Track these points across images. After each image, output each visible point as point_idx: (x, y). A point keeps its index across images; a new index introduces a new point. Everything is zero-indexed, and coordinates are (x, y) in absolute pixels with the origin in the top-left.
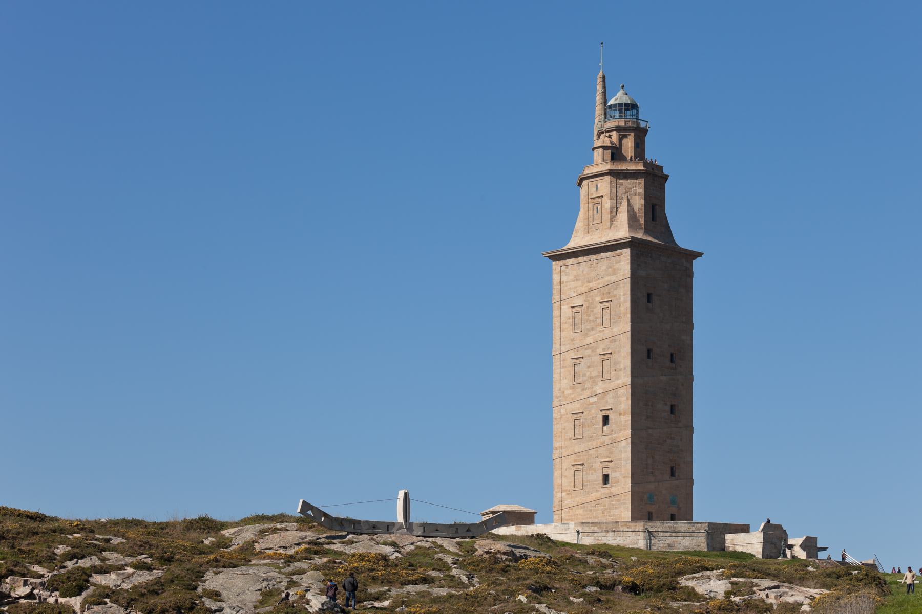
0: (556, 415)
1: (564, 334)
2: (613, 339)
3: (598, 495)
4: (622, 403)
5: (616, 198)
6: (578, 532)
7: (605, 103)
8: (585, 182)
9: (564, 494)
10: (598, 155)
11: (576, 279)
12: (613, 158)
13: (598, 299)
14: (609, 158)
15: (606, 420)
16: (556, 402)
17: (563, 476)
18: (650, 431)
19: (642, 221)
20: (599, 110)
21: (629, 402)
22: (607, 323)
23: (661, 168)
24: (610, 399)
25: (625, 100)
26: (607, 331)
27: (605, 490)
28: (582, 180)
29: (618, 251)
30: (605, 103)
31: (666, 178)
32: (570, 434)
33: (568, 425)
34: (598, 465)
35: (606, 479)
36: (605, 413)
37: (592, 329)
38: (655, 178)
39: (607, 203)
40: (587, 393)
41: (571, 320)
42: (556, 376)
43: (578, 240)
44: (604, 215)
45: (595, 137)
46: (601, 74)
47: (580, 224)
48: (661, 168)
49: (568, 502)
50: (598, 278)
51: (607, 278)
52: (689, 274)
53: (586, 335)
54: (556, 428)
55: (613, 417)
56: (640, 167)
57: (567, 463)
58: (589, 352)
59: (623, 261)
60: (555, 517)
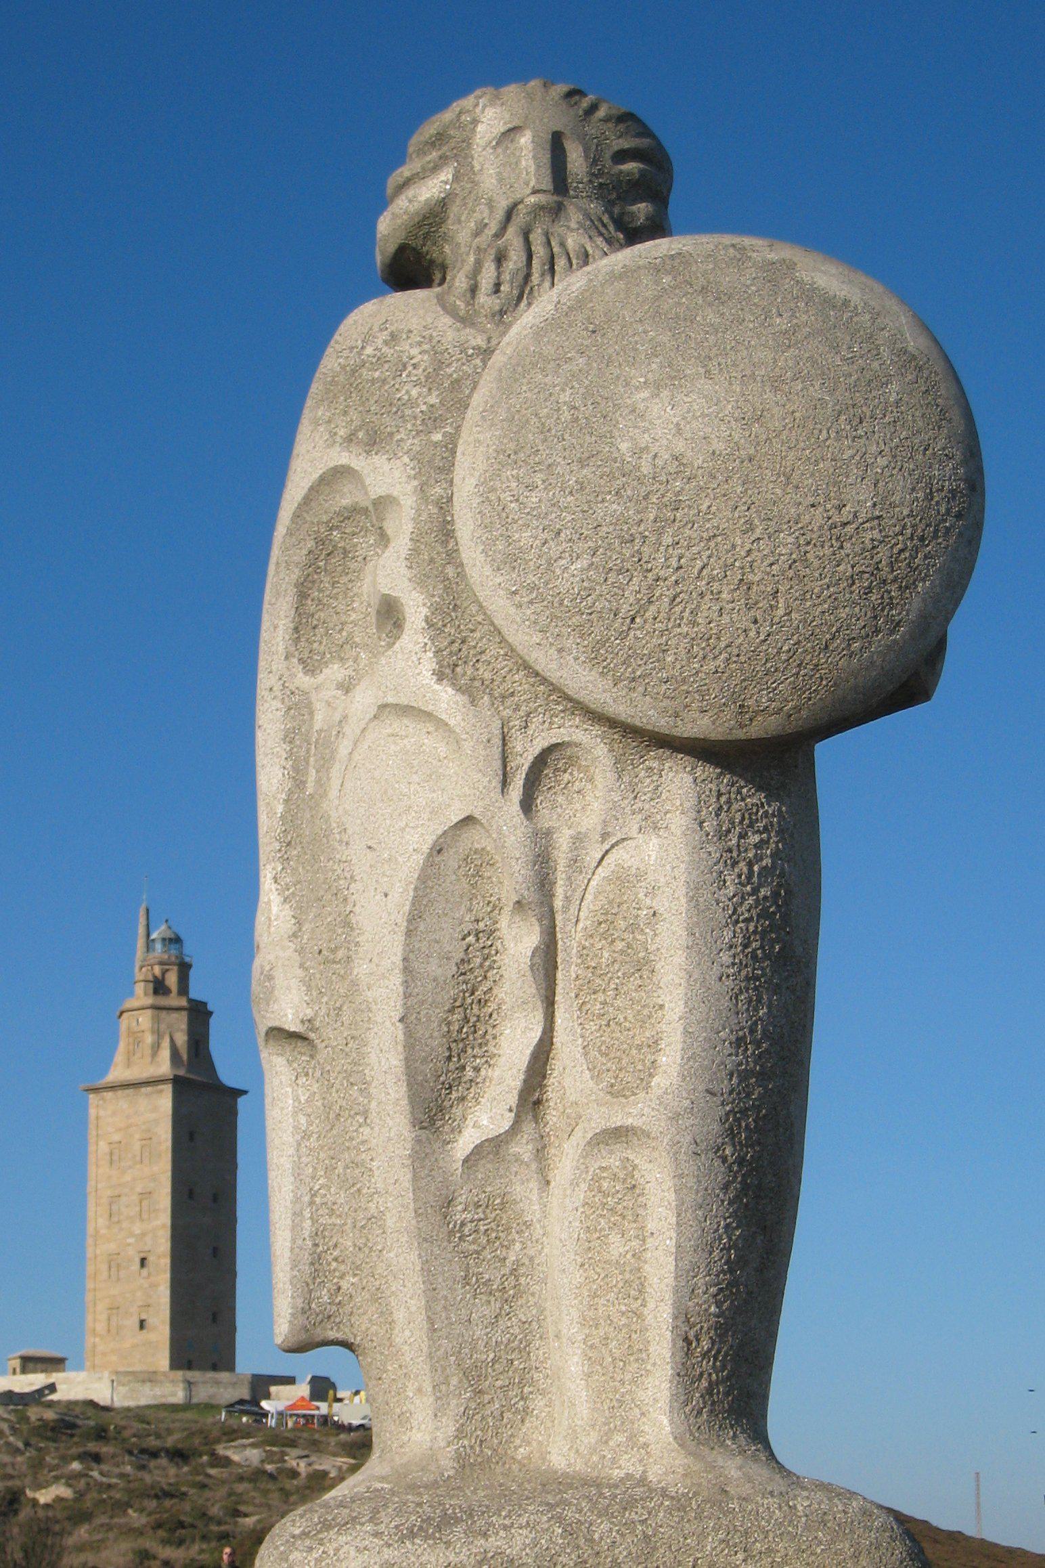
0: (90, 1253)
1: (101, 1171)
2: (153, 1178)
4: (161, 1246)
5: (158, 1035)
7: (148, 935)
8: (125, 1015)
9: (97, 1340)
10: (140, 988)
11: (114, 1114)
12: (156, 992)
13: (137, 1136)
14: (151, 991)
16: (90, 1241)
17: (96, 1319)
19: (185, 1057)
20: (141, 943)
21: (169, 1244)
23: (205, 1004)
24: (148, 1239)
25: (169, 934)
28: (122, 1013)
29: (160, 1087)
30: (148, 935)
31: (211, 1013)
32: (105, 1274)
33: (104, 1267)
34: (134, 1309)
36: (143, 1255)
37: (130, 1167)
38: (199, 1014)
39: (149, 1039)
41: (108, 1157)
42: (91, 1213)
43: (118, 1073)
44: (143, 1048)
45: (137, 969)
46: (144, 906)
47: (119, 1057)
48: (205, 1004)
49: (100, 1348)
52: (234, 1113)
54: (90, 1269)
55: (151, 1259)
56: (183, 1002)
57: (101, 1306)
59: (164, 1101)
60: (88, 1364)
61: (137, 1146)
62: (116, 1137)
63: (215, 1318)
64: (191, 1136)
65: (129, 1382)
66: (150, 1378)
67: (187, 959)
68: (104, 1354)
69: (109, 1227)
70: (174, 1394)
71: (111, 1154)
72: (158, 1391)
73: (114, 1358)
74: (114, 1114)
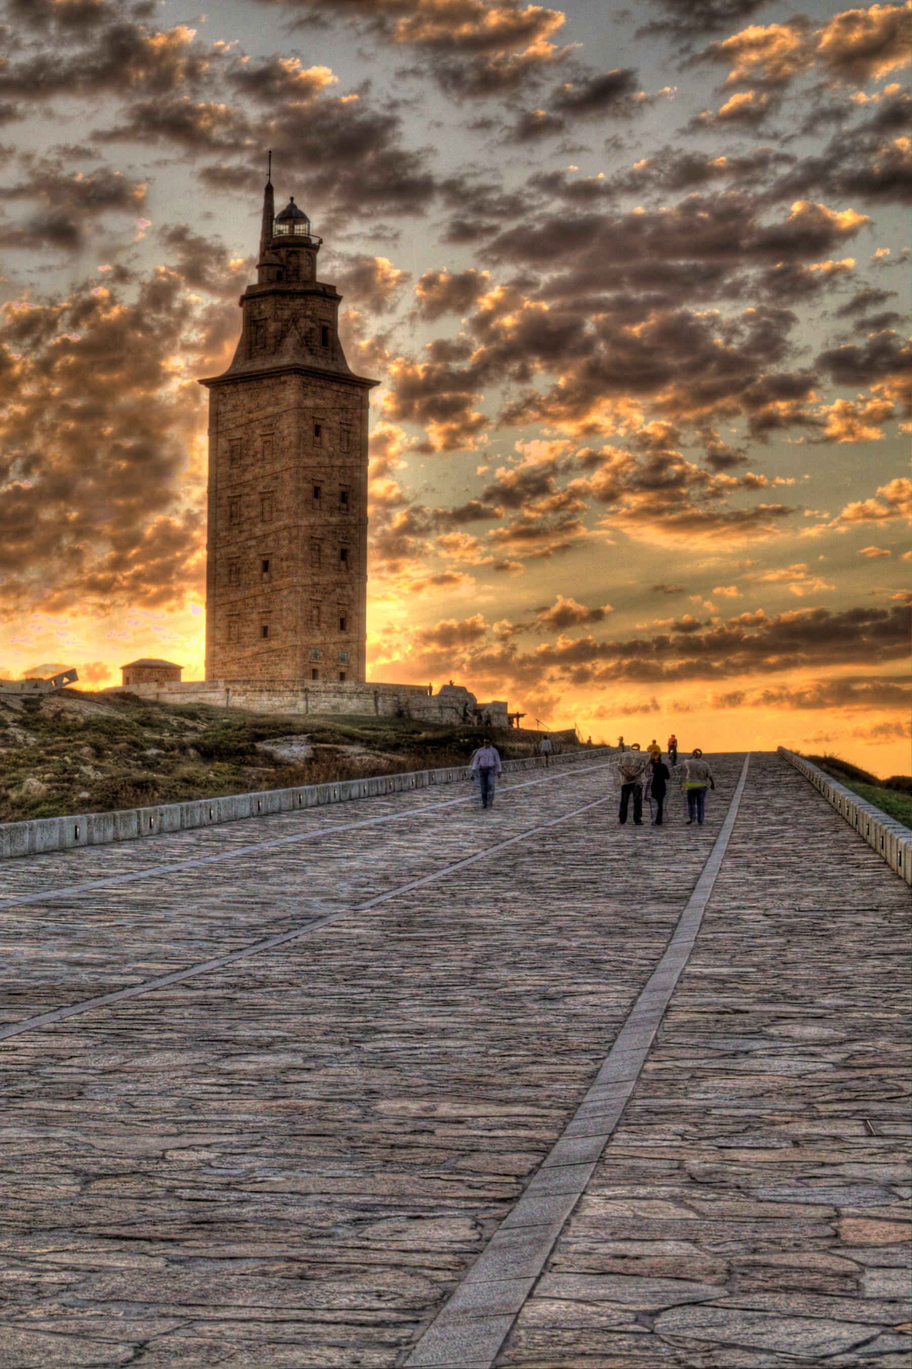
3: (256, 649)
6: (228, 690)
11: (235, 408)
12: (279, 274)
13: (259, 432)
15: (266, 566)
18: (316, 579)
22: (268, 457)
26: (268, 467)
27: (264, 645)
32: (225, 579)
35: (265, 632)
40: (245, 535)
50: (259, 407)
51: (270, 409)
53: (245, 471)
55: (274, 562)
58: (247, 490)
61: (258, 444)
62: (238, 434)
63: (343, 625)
64: (317, 430)
65: (245, 691)
66: (271, 686)
67: (315, 241)
68: (224, 664)
69: (229, 529)
70: (294, 705)
71: (232, 452)
72: (276, 701)
73: (235, 668)
74: (235, 408)
